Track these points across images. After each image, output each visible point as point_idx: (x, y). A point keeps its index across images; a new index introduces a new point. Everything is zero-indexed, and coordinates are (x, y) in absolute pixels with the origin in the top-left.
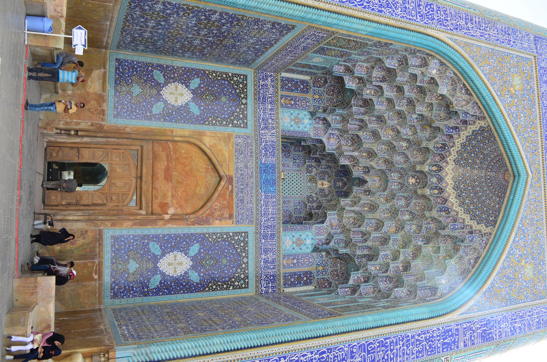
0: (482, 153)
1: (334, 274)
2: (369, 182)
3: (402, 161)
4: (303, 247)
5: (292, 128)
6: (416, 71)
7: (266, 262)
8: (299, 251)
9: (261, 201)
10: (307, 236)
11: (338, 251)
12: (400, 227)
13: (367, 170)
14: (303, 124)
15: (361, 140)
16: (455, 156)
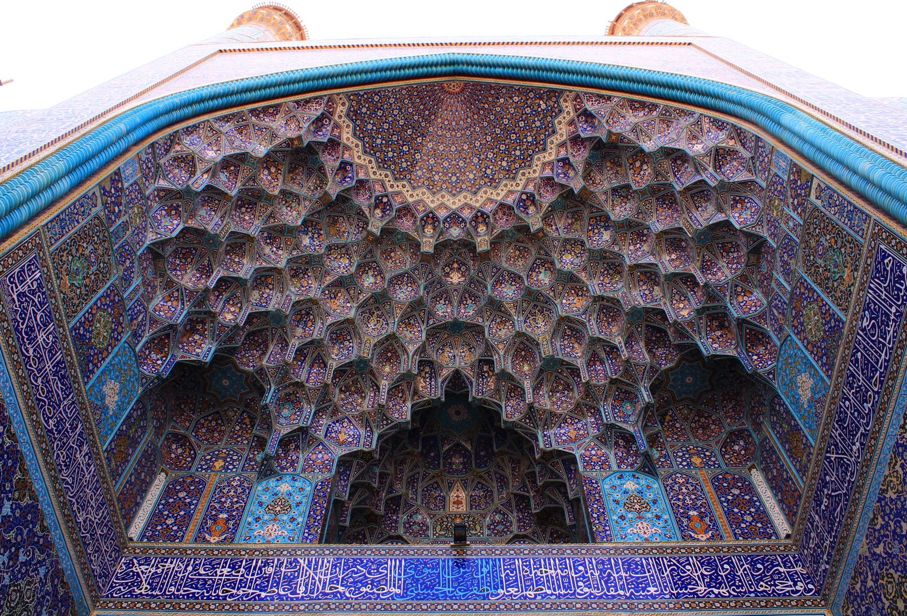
0: (403, 129)
1: (704, 434)
2: (457, 365)
3: (410, 289)
4: (649, 496)
5: (300, 520)
6: (200, 182)
7: (714, 581)
8: (663, 504)
9: (525, 597)
10: (614, 487)
11: (648, 407)
12: (570, 282)
13: (427, 369)
14: (290, 494)
15: (350, 364)
16: (404, 186)
